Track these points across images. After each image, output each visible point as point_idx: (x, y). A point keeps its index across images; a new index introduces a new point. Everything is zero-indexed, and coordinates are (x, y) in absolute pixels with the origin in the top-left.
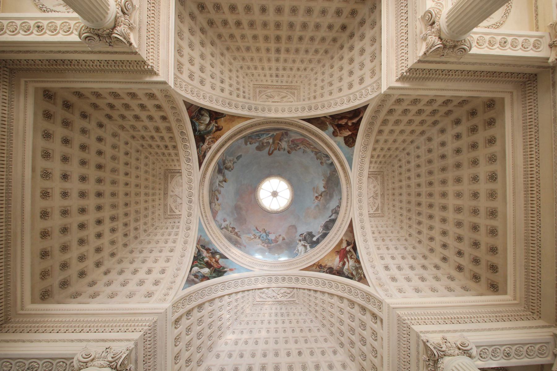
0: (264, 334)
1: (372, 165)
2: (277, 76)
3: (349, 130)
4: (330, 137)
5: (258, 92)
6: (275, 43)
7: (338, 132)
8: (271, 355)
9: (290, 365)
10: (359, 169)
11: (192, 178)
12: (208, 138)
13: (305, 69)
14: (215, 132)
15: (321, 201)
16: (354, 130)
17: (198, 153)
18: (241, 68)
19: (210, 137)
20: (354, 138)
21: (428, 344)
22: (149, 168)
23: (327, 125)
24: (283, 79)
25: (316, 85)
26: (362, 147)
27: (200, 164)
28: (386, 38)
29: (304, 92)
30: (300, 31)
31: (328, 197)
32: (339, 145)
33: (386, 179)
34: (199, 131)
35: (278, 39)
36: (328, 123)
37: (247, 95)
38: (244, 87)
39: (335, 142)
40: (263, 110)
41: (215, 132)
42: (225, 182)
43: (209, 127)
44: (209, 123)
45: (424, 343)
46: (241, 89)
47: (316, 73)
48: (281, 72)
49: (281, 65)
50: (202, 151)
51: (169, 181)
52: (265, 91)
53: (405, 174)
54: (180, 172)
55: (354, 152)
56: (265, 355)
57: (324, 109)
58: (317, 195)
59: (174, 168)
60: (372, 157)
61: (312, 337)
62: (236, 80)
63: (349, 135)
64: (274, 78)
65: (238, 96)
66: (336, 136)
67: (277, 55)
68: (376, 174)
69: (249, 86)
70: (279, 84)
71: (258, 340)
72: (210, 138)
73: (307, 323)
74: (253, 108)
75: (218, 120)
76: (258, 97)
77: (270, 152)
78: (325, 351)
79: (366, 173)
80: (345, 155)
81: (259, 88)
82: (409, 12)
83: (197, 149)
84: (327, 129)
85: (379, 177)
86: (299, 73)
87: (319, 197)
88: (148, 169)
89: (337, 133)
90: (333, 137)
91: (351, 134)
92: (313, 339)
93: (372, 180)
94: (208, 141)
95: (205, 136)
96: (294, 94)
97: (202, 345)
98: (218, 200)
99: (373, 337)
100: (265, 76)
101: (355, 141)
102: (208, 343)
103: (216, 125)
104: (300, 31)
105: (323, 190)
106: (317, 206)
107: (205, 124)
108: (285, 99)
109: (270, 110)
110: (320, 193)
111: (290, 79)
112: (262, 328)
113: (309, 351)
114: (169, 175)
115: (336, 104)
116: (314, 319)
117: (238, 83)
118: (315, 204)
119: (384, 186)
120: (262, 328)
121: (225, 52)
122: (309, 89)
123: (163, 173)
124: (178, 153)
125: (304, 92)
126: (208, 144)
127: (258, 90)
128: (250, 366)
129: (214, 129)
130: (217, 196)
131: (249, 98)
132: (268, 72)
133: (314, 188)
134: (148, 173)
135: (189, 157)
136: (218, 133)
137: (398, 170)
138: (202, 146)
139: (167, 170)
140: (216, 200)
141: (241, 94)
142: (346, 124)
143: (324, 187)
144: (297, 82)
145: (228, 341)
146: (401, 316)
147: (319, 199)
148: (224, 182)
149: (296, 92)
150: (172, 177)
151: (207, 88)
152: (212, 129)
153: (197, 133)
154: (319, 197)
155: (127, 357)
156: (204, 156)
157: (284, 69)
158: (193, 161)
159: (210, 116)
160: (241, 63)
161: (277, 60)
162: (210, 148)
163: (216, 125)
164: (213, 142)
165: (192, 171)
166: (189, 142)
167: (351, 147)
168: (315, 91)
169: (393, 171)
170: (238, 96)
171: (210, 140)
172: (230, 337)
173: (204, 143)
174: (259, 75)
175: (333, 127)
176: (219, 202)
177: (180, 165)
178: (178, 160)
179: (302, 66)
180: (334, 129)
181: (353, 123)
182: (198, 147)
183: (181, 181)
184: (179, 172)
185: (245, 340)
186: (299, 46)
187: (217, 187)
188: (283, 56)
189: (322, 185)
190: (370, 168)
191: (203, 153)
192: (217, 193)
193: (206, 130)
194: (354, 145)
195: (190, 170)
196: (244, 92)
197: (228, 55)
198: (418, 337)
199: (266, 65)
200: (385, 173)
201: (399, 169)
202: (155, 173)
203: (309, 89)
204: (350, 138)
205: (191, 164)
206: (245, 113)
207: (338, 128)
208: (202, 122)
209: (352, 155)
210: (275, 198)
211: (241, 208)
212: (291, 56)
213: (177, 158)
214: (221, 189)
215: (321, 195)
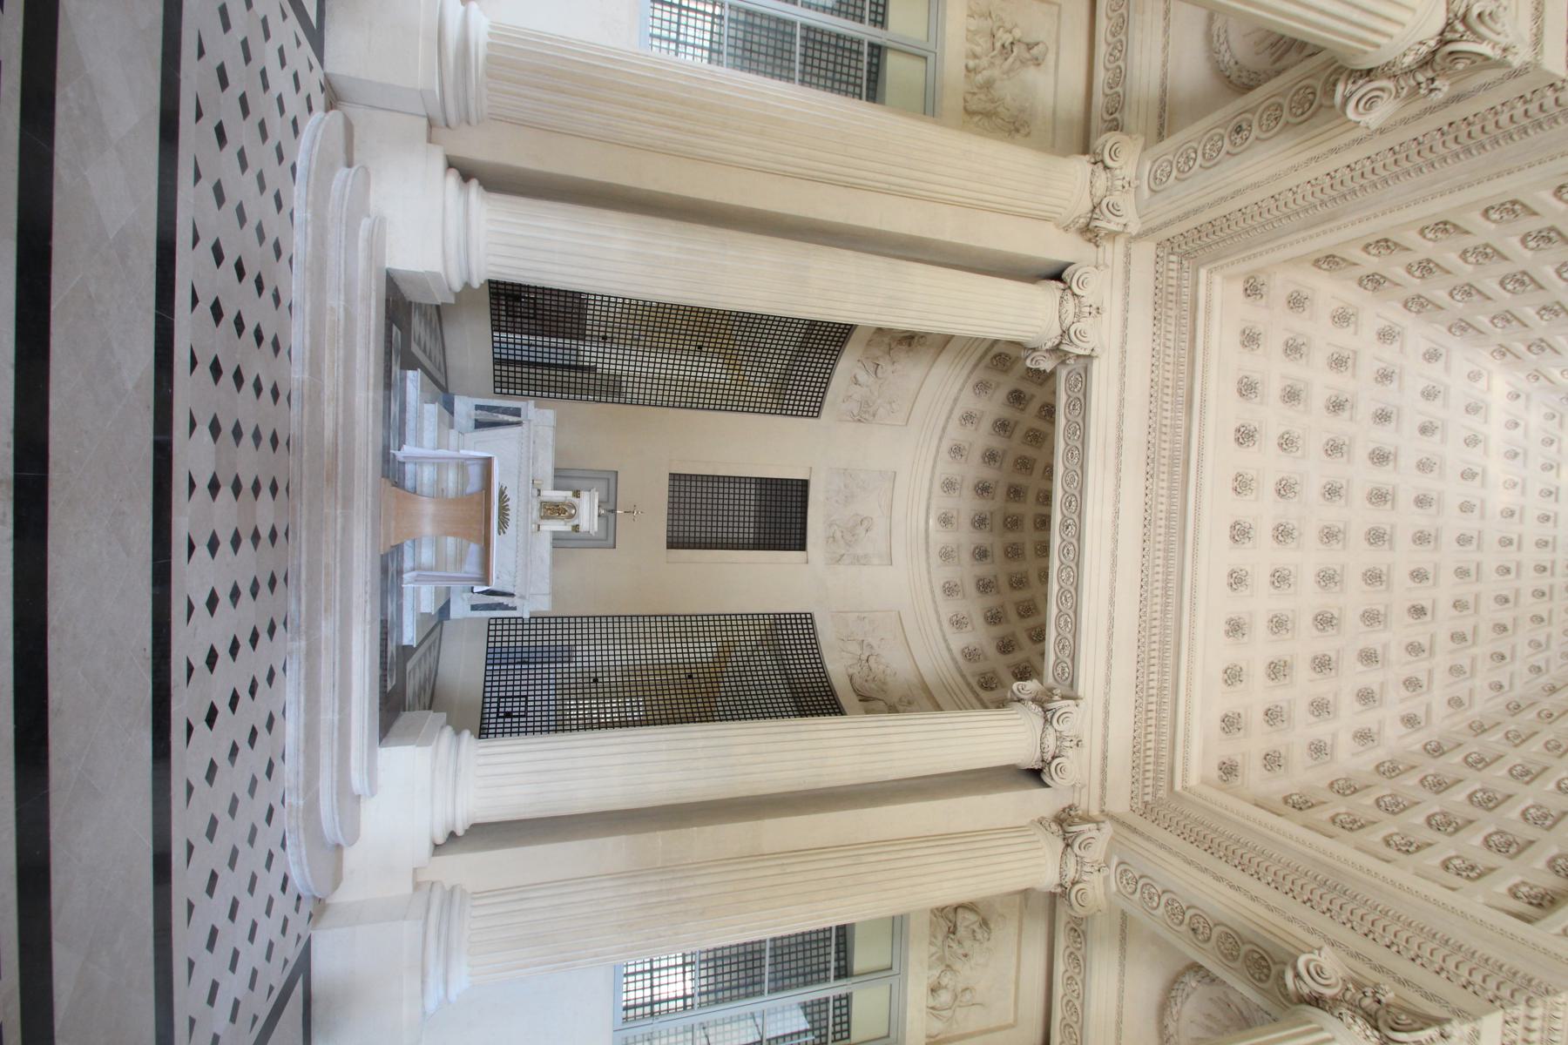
0: (1500, 499)
8: (1420, 520)
9: (1384, 578)
21: (1432, 1032)
45: (1439, 1021)
56: (1422, 501)
61: (1474, 660)
71: (1478, 478)
73: (1528, 650)
78: (1419, 691)
92: (1466, 663)
97: (1476, 297)
99: (1457, 862)
102: (1481, 318)
112: (1523, 492)
113: (1424, 641)
116: (1544, 680)
120: (1523, 492)
128: (1391, 457)
145: (1482, 384)
146: (1549, 999)
155: (1479, 61)
172: (1499, 383)
185: (1480, 437)
198: (1462, 1014)
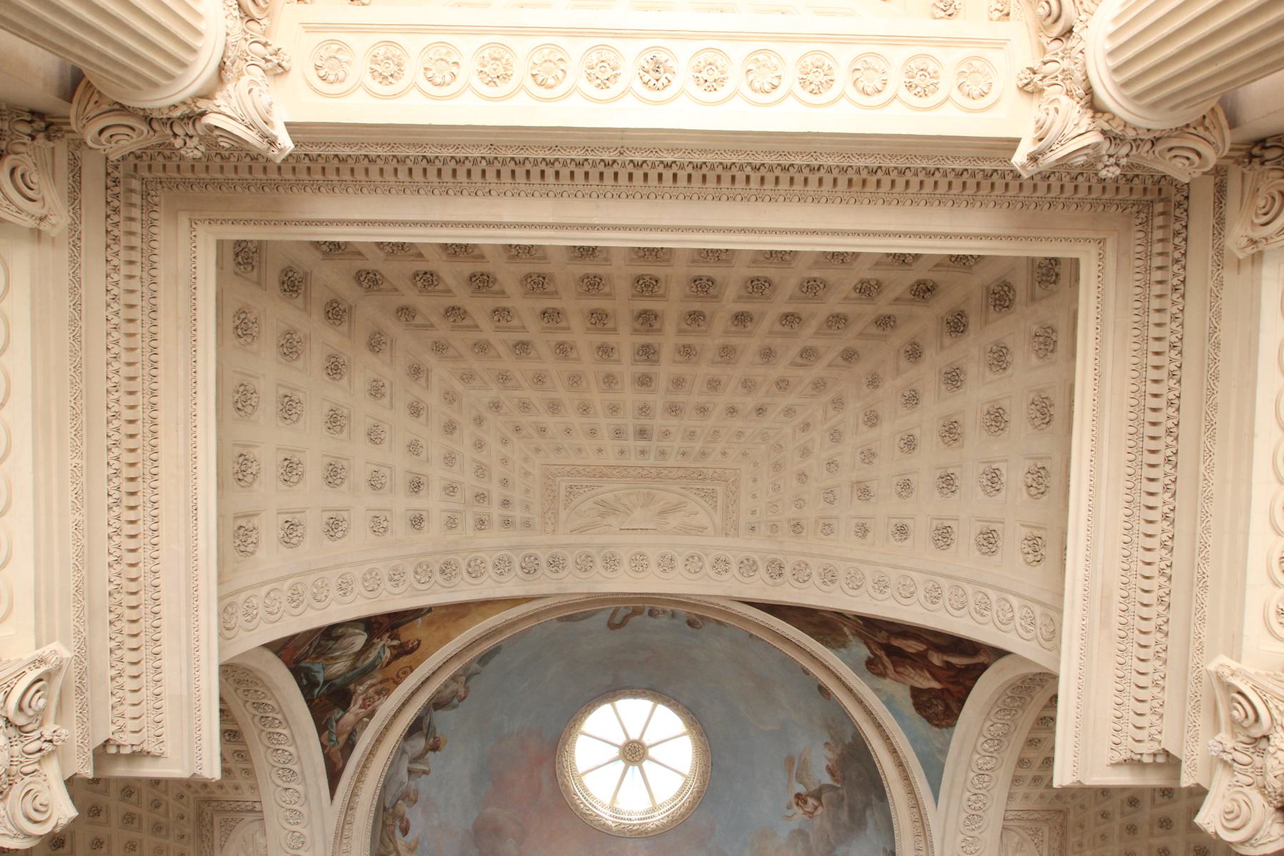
1: (1021, 790)
2: (642, 433)
3: (931, 673)
4: (855, 669)
5: (563, 492)
6: (635, 331)
7: (890, 666)
10: (965, 803)
11: (305, 832)
12: (361, 689)
13: (760, 411)
14: (389, 663)
15: (817, 821)
16: (953, 683)
17: (323, 747)
18: (496, 406)
19: (369, 682)
20: (953, 705)
22: (138, 804)
23: (845, 635)
24: (665, 444)
25: (802, 476)
26: (982, 739)
27: (334, 777)
28: (1081, 573)
29: (754, 496)
30: (740, 298)
31: (844, 816)
32: (889, 703)
33: (1073, 840)
34: (326, 682)
35: (647, 320)
36: (846, 629)
37: (517, 513)
38: (505, 482)
39: (876, 691)
40: (585, 564)
41: (389, 663)
42: (435, 748)
43: (368, 657)
44: (368, 645)
46: (496, 492)
47: (806, 427)
48: (658, 422)
49: (657, 399)
50: (338, 735)
51: (217, 842)
52: (592, 488)
53: (1151, 834)
54: (255, 810)
55: (948, 744)
57: (832, 587)
58: (800, 789)
59: (233, 795)
60: (1022, 762)
62: (474, 460)
63: (931, 690)
64: (632, 443)
65: (481, 523)
66: (883, 675)
67: (642, 368)
68: (1035, 820)
69: (527, 474)
70: (651, 461)
72: (373, 685)
74: (544, 564)
75: (401, 629)
76: (563, 515)
77: (617, 620)
79: (994, 817)
80: (913, 742)
81: (569, 474)
82: (1184, 431)
83: (320, 734)
84: (844, 645)
85: (1046, 829)
86: (737, 423)
87: (811, 801)
88: (133, 809)
89: (885, 667)
90: (869, 675)
91: (941, 690)
93: (1016, 839)
94: (362, 697)
95: (352, 687)
96: (710, 496)
98: (405, 831)
100: (593, 432)
101: (957, 716)
103: (395, 643)
104: (740, 298)
105: (827, 779)
106: (801, 833)
107: (350, 655)
108: (674, 520)
109: (611, 562)
110: (813, 788)
111: (698, 445)
114: (217, 819)
115: (881, 585)
117: (481, 471)
118: (794, 825)
119: (1063, 835)
121: (430, 359)
122: (776, 488)
123: (191, 813)
124: (248, 752)
125: (754, 496)
126: (364, 706)
127: (563, 485)
129: (388, 653)
130: (402, 818)
131: (527, 524)
132: (604, 423)
133: (790, 761)
134: (136, 825)
135: (288, 766)
136: (405, 660)
137: (1122, 814)
138: (337, 721)
139: (208, 801)
140: (398, 833)
141: (496, 511)
142: (922, 656)
143: (831, 771)
144: (724, 454)
147: (809, 808)
148: (430, 755)
149: (720, 489)
150: (229, 828)
151: (358, 539)
152: (379, 657)
153: (317, 690)
154: (811, 801)
156: (350, 746)
157: (674, 410)
158: (304, 778)
159: (366, 630)
160: (494, 392)
161: (644, 381)
162: (371, 715)
163: (395, 643)
164: (384, 692)
165: (304, 810)
166: (288, 726)
167: (937, 726)
168: (799, 502)
169: (1105, 815)
170: (481, 523)
171: (371, 690)
173: (346, 708)
174: (568, 431)
175: (869, 648)
176: (410, 836)
177: (254, 788)
178: (249, 772)
179: (750, 402)
180: (873, 653)
181: (947, 663)
182: (322, 727)
183: (261, 841)
184: (252, 811)
186: (734, 341)
187: (402, 783)
188: (665, 370)
189: (825, 763)
190: (1010, 797)
191: (342, 739)
192: (403, 807)
193: (355, 668)
194: (952, 725)
195: (296, 807)
196: (506, 503)
197: (440, 371)
199: (597, 398)
200: (1071, 817)
201: (1128, 809)
202: (163, 820)
203: (776, 488)
204: (936, 698)
205: (300, 788)
206: (510, 588)
207: (888, 655)
208: (338, 654)
209: (944, 752)
210: (634, 771)
211: (497, 831)
212: (703, 370)
213: (244, 766)
214: (422, 783)
215: (817, 795)
